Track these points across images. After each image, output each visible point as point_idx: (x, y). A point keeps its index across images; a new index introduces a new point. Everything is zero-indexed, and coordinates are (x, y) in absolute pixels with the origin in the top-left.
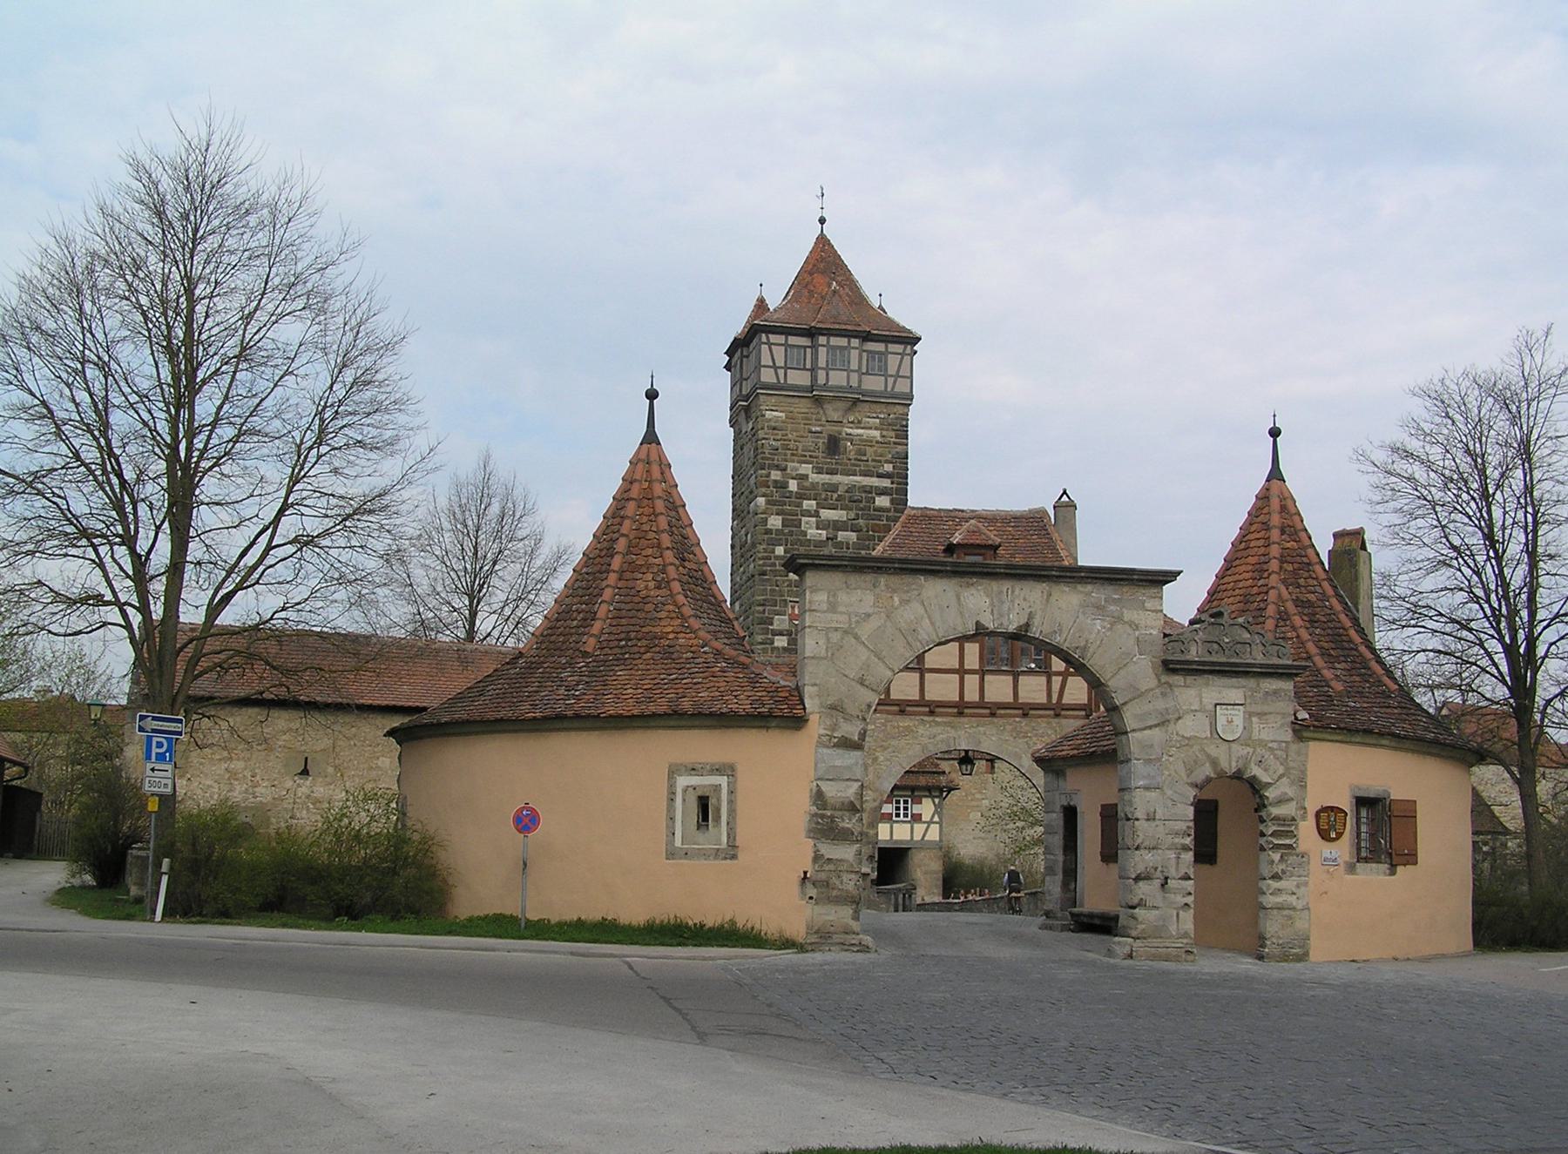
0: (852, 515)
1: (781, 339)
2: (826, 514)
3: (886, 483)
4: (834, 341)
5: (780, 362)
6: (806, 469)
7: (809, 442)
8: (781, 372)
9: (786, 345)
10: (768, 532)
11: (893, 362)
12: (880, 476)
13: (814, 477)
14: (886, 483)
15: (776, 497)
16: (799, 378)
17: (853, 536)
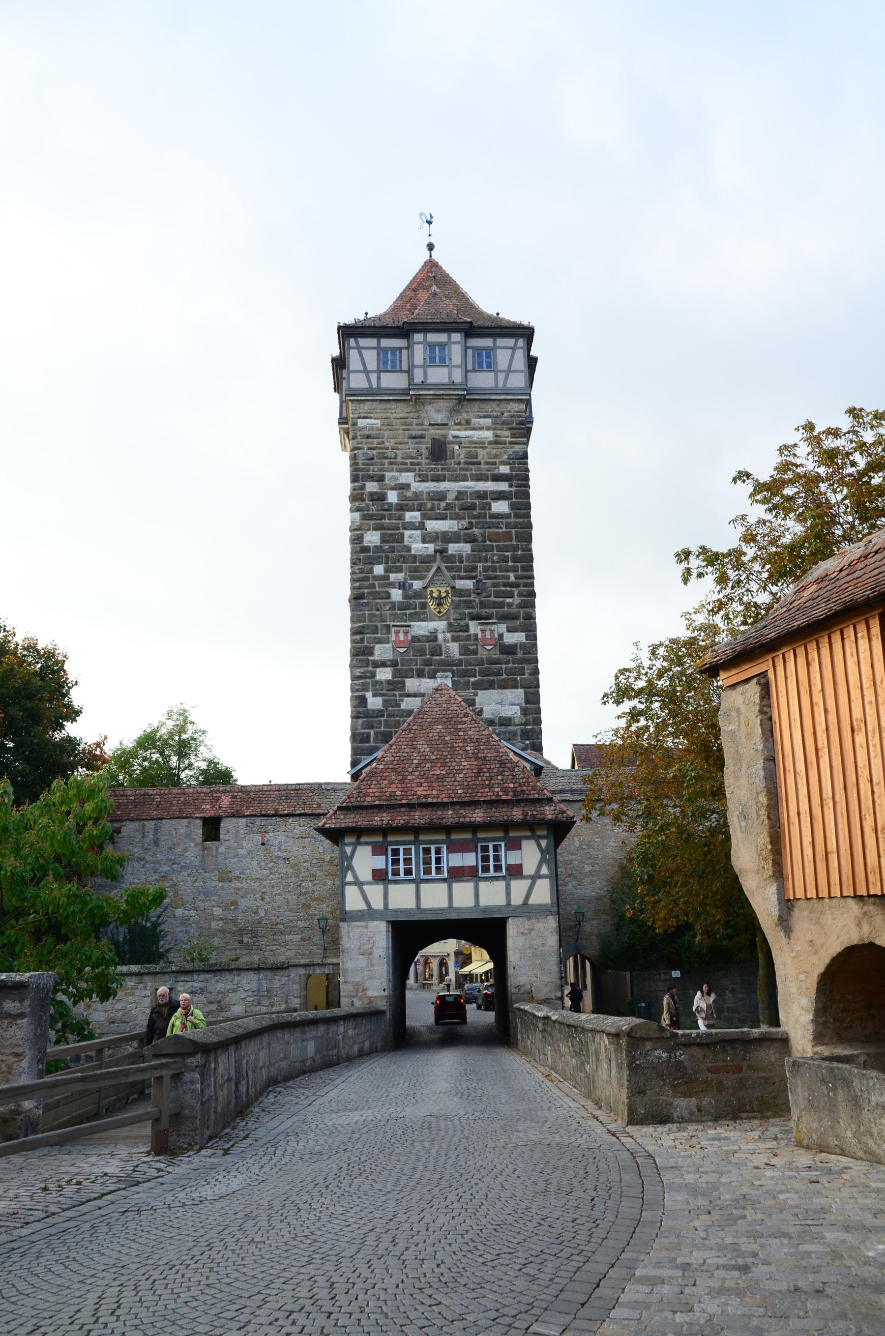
0: (465, 523)
1: (372, 342)
2: (433, 525)
3: (503, 486)
4: (433, 337)
5: (372, 365)
6: (406, 477)
7: (411, 447)
8: (373, 378)
9: (378, 348)
10: (365, 549)
11: (502, 358)
12: (497, 478)
13: (418, 486)
14: (503, 486)
15: (373, 510)
16: (394, 381)
17: (466, 548)
